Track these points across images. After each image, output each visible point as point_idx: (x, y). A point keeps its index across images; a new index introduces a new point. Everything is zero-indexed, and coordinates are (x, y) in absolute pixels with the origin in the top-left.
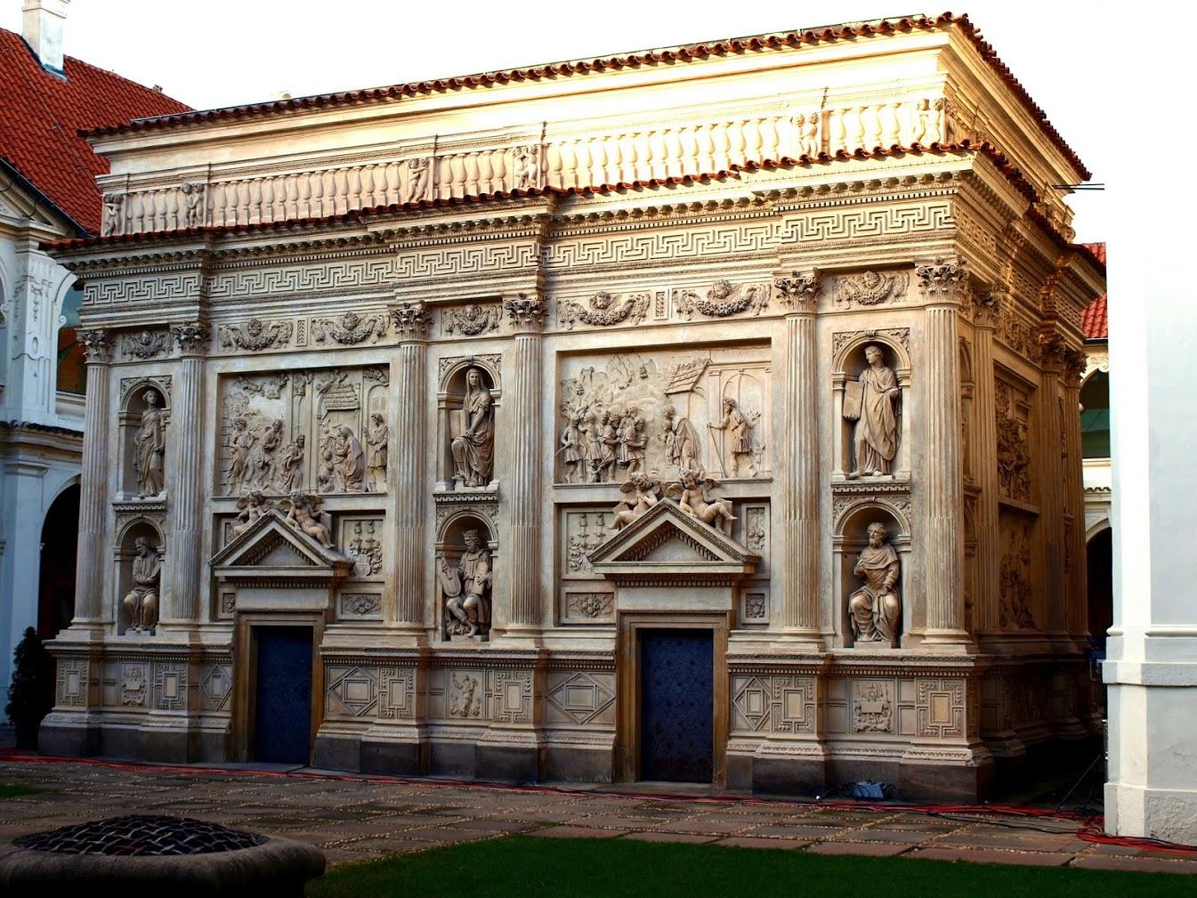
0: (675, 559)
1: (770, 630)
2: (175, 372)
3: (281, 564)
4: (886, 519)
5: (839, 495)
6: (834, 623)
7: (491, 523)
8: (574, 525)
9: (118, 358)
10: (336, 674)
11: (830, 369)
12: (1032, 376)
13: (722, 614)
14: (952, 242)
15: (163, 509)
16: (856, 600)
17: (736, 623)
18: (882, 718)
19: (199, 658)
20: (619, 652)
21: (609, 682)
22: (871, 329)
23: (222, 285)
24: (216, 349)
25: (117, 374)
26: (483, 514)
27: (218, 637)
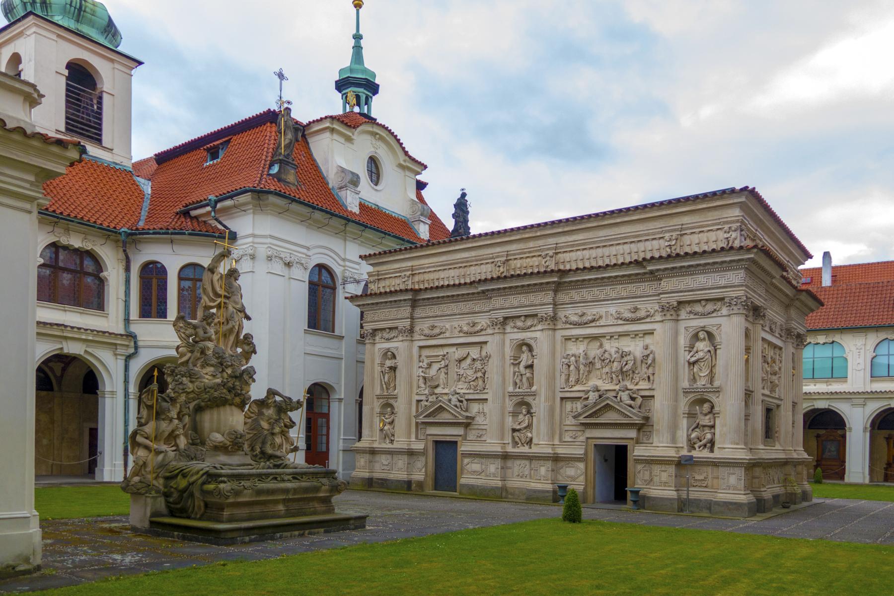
2: (398, 345)
3: (444, 417)
5: (686, 392)
8: (569, 406)
9: (377, 341)
12: (779, 343)
15: (395, 397)
17: (638, 442)
23: (419, 312)
24: (416, 336)
25: (378, 346)
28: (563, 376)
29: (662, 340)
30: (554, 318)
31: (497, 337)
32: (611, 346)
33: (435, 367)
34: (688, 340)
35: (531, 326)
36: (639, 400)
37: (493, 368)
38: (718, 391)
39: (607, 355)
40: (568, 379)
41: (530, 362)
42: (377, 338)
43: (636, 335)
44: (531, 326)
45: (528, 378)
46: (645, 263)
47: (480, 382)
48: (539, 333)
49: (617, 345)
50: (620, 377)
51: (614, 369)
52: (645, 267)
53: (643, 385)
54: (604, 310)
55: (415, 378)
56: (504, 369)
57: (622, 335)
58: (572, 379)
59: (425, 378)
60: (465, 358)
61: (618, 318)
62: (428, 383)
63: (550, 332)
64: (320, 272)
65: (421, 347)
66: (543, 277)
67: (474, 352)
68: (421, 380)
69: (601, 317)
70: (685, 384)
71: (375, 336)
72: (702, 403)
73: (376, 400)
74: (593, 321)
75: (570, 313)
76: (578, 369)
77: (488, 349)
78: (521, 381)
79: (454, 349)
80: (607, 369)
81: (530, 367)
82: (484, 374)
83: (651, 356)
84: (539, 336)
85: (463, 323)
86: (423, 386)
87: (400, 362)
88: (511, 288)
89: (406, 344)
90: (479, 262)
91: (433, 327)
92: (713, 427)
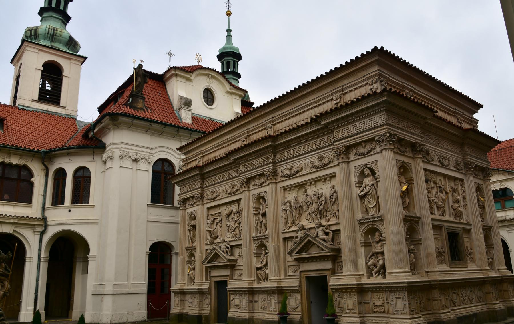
0: (313, 252)
1: (343, 274)
4: (377, 230)
6: (363, 270)
7: (267, 244)
10: (232, 296)
11: (354, 178)
13: (328, 270)
14: (386, 127)
16: (370, 263)
18: (382, 307)
19: (201, 292)
20: (300, 286)
21: (298, 296)
22: (365, 163)
23: (207, 183)
24: (205, 201)
26: (265, 242)
27: (206, 286)
28: (283, 219)
29: (342, 180)
30: (275, 174)
31: (245, 194)
32: (311, 190)
33: (216, 221)
34: (357, 178)
35: (263, 182)
36: (331, 233)
37: (244, 219)
38: (381, 220)
39: (308, 199)
40: (287, 222)
41: (264, 211)
42: (187, 205)
44: (263, 182)
45: (264, 224)
47: (237, 231)
48: (268, 187)
49: (314, 189)
50: (318, 216)
53: (333, 221)
55: (205, 232)
56: (250, 219)
57: (317, 180)
59: (210, 232)
60: (230, 214)
61: (312, 167)
62: (213, 236)
63: (273, 185)
64: (163, 165)
65: (209, 209)
66: (263, 144)
67: (235, 208)
68: (208, 234)
69: (302, 168)
70: (359, 216)
71: (186, 204)
72: (372, 231)
73: (186, 252)
74: (297, 172)
75: (284, 169)
76: (292, 213)
77: (242, 203)
78: (261, 227)
80: (309, 211)
81: (264, 215)
82: (240, 224)
83: (335, 194)
84: (268, 190)
85: (227, 187)
86: (209, 238)
87: (197, 221)
88: (248, 155)
89: (199, 207)
91: (213, 192)
92: (383, 253)
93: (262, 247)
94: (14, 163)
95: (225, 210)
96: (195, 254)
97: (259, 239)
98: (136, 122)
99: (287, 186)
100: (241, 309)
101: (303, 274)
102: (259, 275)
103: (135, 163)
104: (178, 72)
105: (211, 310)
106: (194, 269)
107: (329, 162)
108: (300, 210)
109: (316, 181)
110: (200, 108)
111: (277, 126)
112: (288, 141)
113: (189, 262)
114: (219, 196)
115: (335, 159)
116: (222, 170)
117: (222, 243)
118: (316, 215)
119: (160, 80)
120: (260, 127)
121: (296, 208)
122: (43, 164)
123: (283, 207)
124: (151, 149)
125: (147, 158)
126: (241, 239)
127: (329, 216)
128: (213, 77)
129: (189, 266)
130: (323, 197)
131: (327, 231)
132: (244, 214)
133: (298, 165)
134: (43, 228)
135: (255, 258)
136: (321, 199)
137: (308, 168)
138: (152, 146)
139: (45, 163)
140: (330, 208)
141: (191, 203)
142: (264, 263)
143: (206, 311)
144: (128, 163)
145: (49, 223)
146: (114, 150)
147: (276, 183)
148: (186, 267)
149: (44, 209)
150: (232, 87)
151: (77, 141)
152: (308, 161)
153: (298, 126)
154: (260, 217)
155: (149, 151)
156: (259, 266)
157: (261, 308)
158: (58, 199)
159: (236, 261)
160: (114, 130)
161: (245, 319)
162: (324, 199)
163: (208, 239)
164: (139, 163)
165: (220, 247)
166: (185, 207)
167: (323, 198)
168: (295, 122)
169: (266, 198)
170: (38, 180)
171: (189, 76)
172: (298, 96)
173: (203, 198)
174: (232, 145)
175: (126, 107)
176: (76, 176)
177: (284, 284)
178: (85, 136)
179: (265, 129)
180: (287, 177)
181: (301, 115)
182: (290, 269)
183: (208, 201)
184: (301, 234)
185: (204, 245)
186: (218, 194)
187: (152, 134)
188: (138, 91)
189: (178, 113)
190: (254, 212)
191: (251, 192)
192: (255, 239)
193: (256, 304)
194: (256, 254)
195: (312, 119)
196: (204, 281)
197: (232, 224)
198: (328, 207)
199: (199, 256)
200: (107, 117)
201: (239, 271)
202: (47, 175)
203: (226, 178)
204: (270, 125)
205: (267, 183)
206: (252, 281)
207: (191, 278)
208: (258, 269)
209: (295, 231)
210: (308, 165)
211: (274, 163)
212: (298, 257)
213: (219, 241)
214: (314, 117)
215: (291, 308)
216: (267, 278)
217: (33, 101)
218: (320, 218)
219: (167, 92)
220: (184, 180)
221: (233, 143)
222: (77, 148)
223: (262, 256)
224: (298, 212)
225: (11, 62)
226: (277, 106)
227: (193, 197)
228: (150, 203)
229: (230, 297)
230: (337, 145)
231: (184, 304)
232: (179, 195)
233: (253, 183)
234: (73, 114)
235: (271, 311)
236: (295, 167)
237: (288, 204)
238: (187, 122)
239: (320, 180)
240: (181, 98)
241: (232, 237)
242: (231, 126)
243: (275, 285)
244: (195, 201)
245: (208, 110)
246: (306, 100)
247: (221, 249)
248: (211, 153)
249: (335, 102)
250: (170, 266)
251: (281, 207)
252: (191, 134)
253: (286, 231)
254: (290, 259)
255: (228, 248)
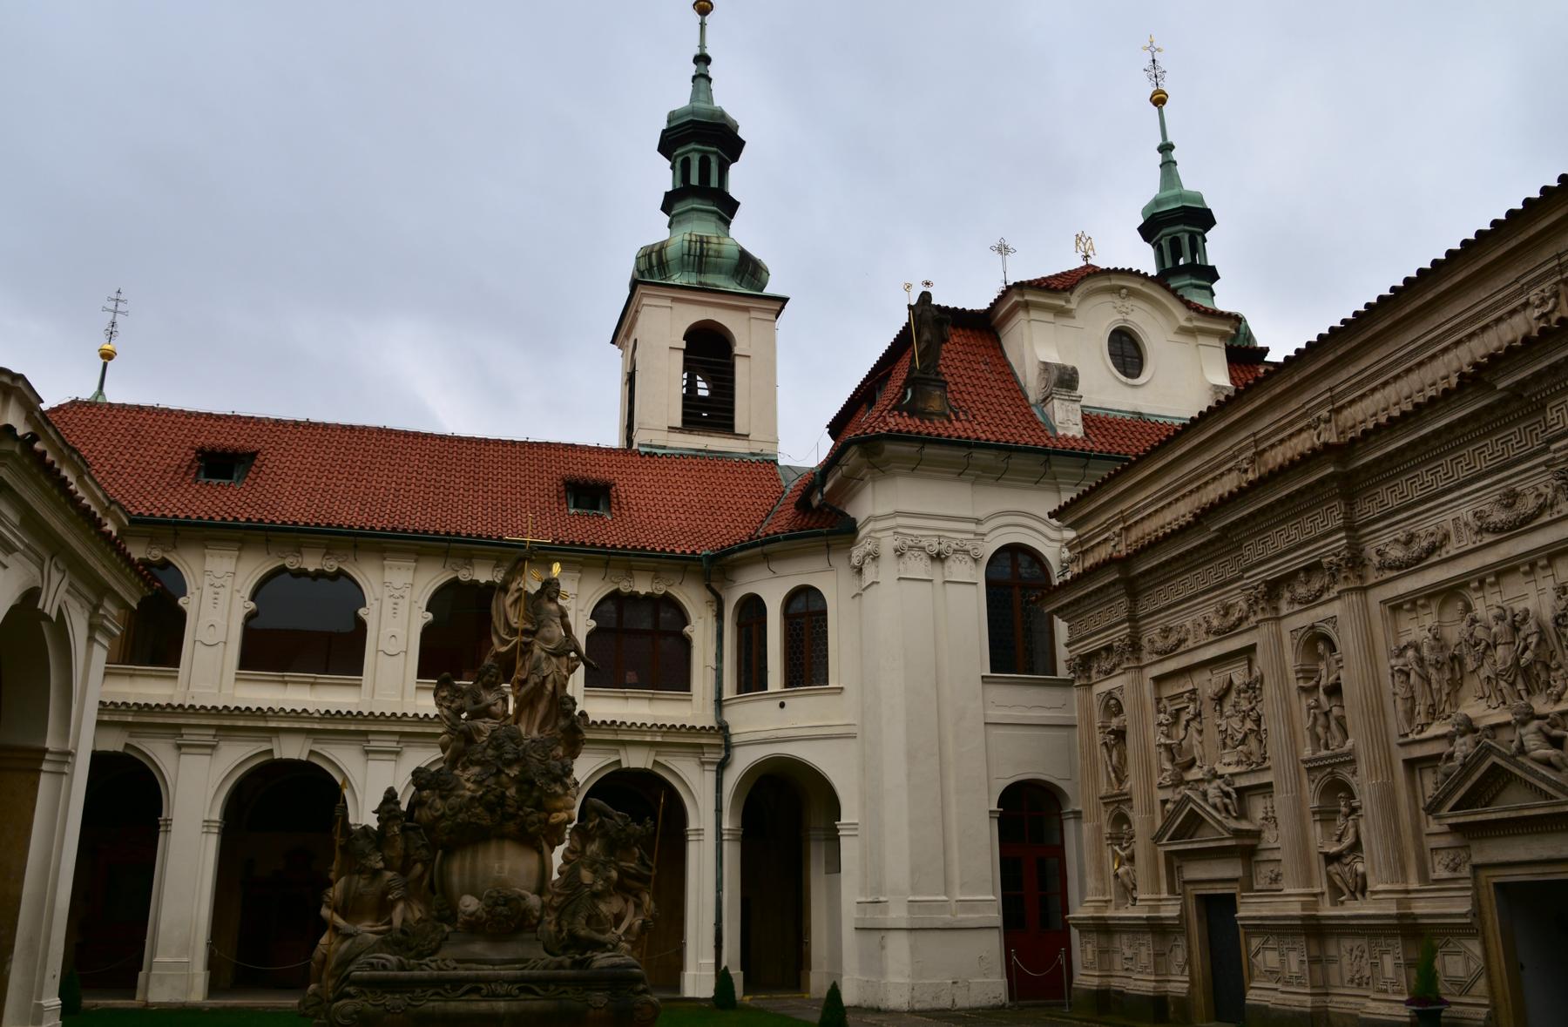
10: (1255, 943)
19: (1156, 928)
20: (1477, 912)
21: (1475, 947)
23: (1146, 605)
26: (1345, 774)
27: (1170, 911)
30: (1356, 561)
31: (1265, 629)
32: (1485, 605)
33: (1184, 717)
35: (1322, 591)
39: (1480, 633)
40: (1412, 710)
42: (1093, 672)
43: (1531, 564)
44: (1322, 591)
46: (1486, 377)
47: (1253, 743)
49: (1496, 599)
50: (1520, 686)
51: (1500, 667)
52: (1492, 388)
54: (1450, 517)
55: (1154, 750)
56: (1289, 705)
57: (1503, 571)
58: (1421, 708)
59: (1168, 748)
61: (1480, 531)
62: (1179, 760)
64: (1015, 565)
65: (1159, 680)
66: (1307, 473)
67: (1238, 674)
68: (1164, 755)
69: (1446, 536)
71: (1090, 669)
74: (1432, 549)
75: (1385, 542)
77: (1260, 659)
78: (1327, 728)
79: (1206, 675)
80: (1486, 671)
81: (1335, 691)
82: (1258, 721)
84: (1336, 611)
86: (1168, 766)
87: (1128, 719)
88: (1261, 511)
90: (1215, 472)
91: (1166, 631)
93: (1335, 791)
94: (642, 592)
95: (1208, 683)
96: (1131, 815)
97: (1326, 766)
98: (930, 450)
99: (1401, 596)
100: (1287, 983)
101: (1483, 874)
102: (1337, 878)
103: (938, 566)
104: (1030, 297)
105: (1192, 982)
106: (1131, 859)
107: (1541, 509)
108: (1452, 670)
109: (1499, 575)
110: (1104, 389)
111: (1346, 413)
112: (1389, 456)
113: (1116, 839)
114: (1185, 640)
115: (1561, 496)
116: (1188, 562)
117: (1209, 782)
118: (1513, 684)
119: (983, 327)
120: (1291, 423)
121: (1439, 665)
122: (709, 587)
123: (1393, 662)
124: (978, 521)
125: (968, 547)
126: (1269, 768)
127: (1560, 684)
128: (1132, 293)
129: (1114, 852)
130: (1531, 622)
131: (1556, 732)
132: (1269, 690)
133: (1432, 529)
134: (723, 755)
135: (1318, 826)
136: (1525, 629)
137: (1466, 533)
138: (980, 514)
139: (713, 585)
140: (1559, 657)
141: (1106, 665)
142: (1347, 841)
143: (1178, 985)
144: (918, 566)
145: (734, 740)
146: (878, 535)
147: (1364, 590)
148: (1108, 853)
149: (719, 703)
150: (1194, 314)
151: (781, 522)
152: (1465, 512)
153: (1417, 406)
154: (1323, 697)
155: (972, 527)
156: (1335, 849)
157: (1352, 981)
158: (752, 678)
159: (1257, 834)
160: (873, 480)
161: (1302, 1014)
162: (1534, 629)
163: (1163, 770)
164: (949, 563)
165: (1205, 795)
166: (1089, 678)
167: (1531, 626)
168: (1406, 392)
169: (1335, 639)
170: (700, 630)
171: (1062, 303)
172: (1408, 310)
173: (1140, 649)
174: (1210, 487)
175: (900, 415)
176: (791, 611)
177: (1420, 908)
178: (803, 504)
179: (1309, 427)
180: (1399, 568)
181: (1423, 370)
182: (1437, 859)
183: (1155, 658)
184: (1463, 747)
185: (1155, 789)
186: (1182, 635)
187: (976, 481)
188: (927, 367)
189: (1043, 413)
190: (1301, 683)
191: (1285, 622)
192: (1313, 767)
193: (1335, 967)
194: (1319, 812)
195: (1462, 376)
196: (1165, 895)
197: (1235, 723)
198: (1552, 656)
199: (1142, 822)
200: (854, 448)
201: (1271, 866)
202: (719, 616)
203: (1202, 588)
204: (1324, 413)
205: (1333, 593)
206: (1315, 895)
207: (1124, 886)
208: (1330, 859)
209: (1443, 736)
210: (1466, 524)
211: (1350, 527)
212: (1461, 820)
213: (1200, 776)
214: (1469, 370)
215: (1453, 983)
216: (1360, 888)
217: (672, 429)
218: (1528, 693)
219: (1002, 356)
220: (1077, 601)
221: (1214, 479)
222: (786, 538)
223: (1340, 820)
224: (1447, 676)
225: (613, 342)
226: (1339, 352)
227: (1108, 649)
228: (987, 673)
229: (1248, 944)
230: (1560, 449)
231: (1111, 962)
232: (1067, 645)
233: (1287, 595)
234: (767, 449)
235: (1386, 991)
236: (1423, 534)
237: (1410, 653)
238: (1070, 434)
239: (1513, 570)
240: (1046, 367)
241: (1239, 763)
242: (1201, 431)
243: (1393, 910)
244: (1115, 660)
245: (1129, 391)
246: (1438, 319)
247: (1206, 800)
248: (1150, 515)
249: (1537, 313)
250: (1060, 851)
251: (1386, 665)
252: (1085, 467)
253: (1411, 737)
254: (1434, 827)
255: (1227, 795)
